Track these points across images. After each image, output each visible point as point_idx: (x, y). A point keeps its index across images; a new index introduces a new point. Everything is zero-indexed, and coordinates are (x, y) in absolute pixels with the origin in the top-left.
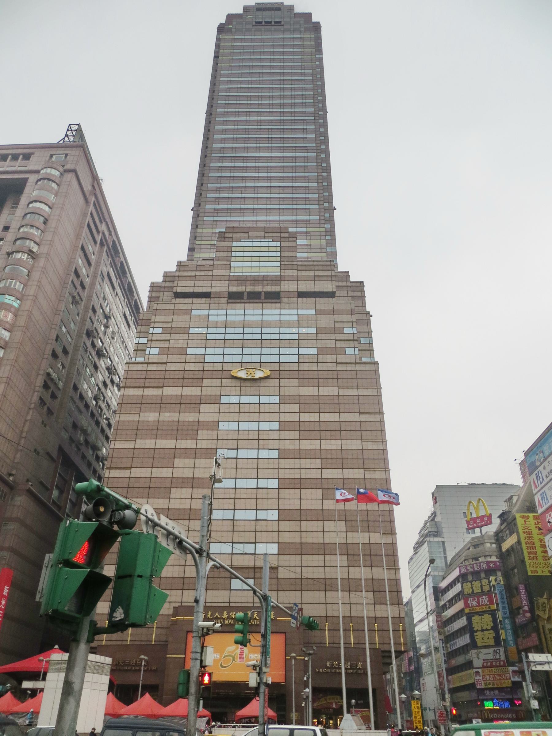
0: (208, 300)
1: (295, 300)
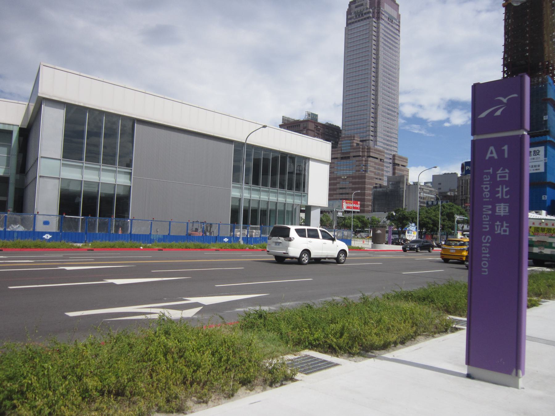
1: (352, 158)
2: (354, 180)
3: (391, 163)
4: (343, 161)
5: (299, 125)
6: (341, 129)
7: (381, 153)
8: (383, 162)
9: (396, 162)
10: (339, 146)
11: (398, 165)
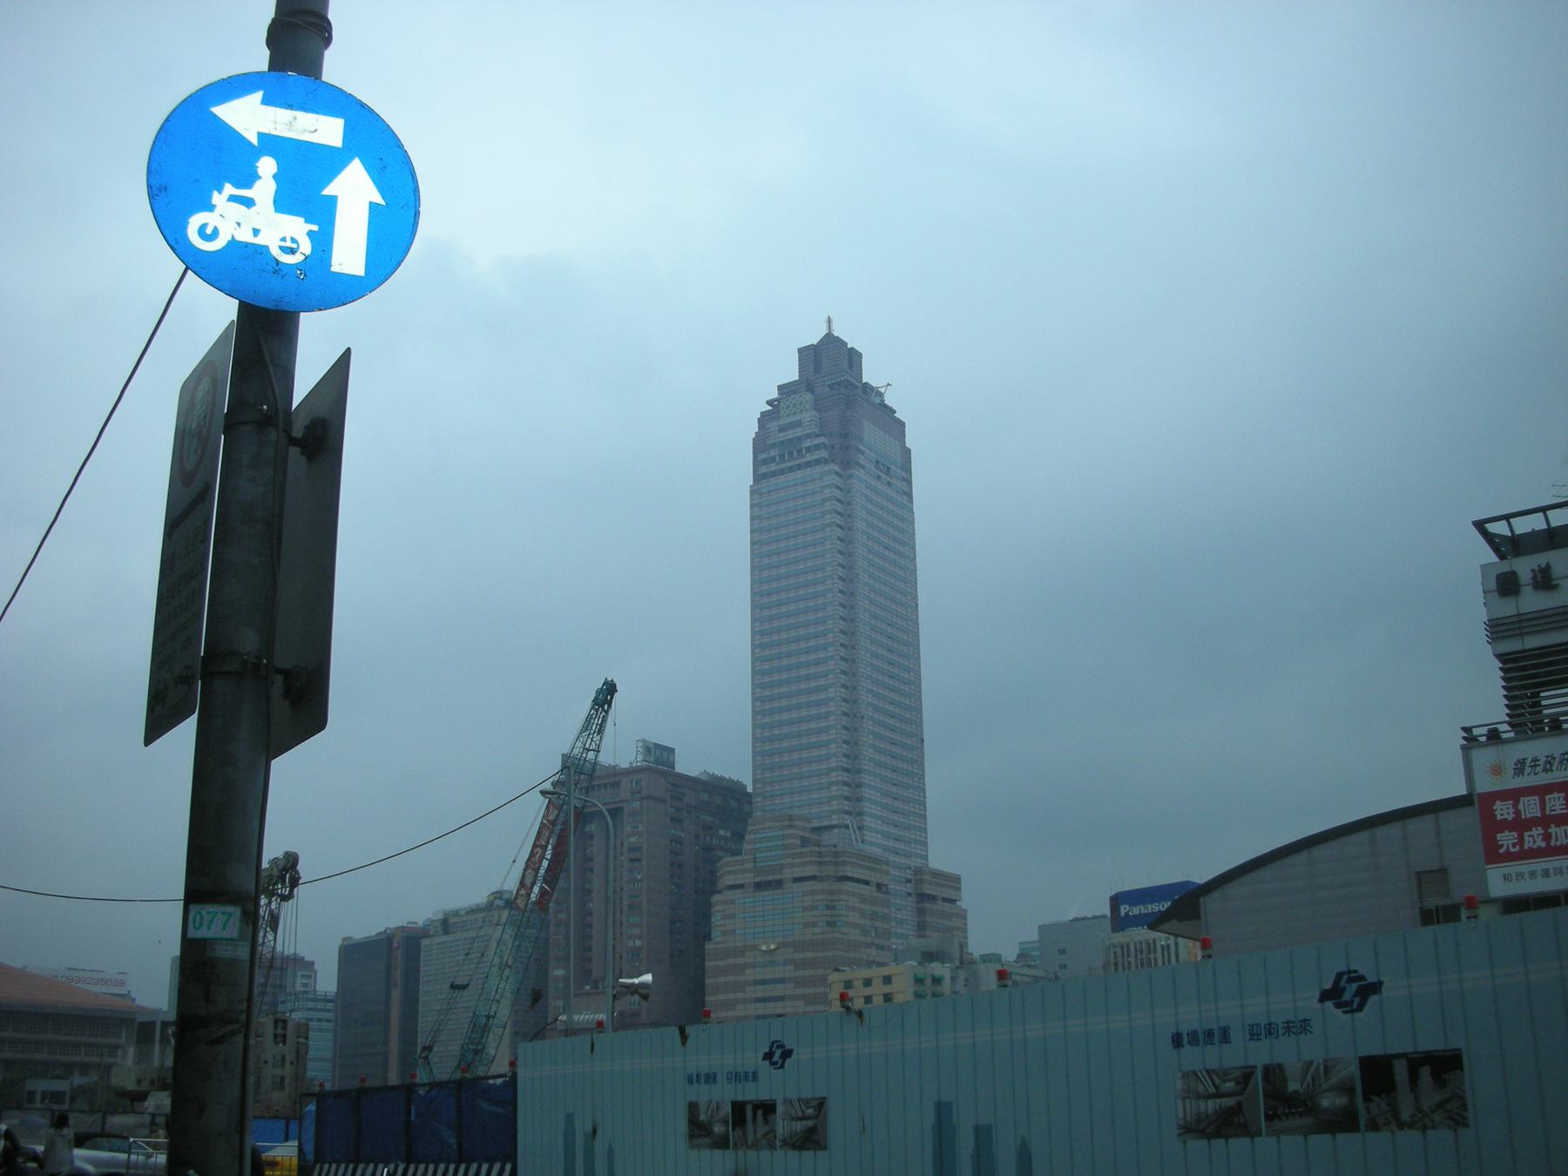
0: (741, 891)
2: (799, 956)
3: (910, 895)
4: (760, 893)
5: (618, 784)
6: (750, 789)
7: (878, 866)
8: (887, 893)
9: (928, 889)
10: (746, 847)
11: (933, 898)
